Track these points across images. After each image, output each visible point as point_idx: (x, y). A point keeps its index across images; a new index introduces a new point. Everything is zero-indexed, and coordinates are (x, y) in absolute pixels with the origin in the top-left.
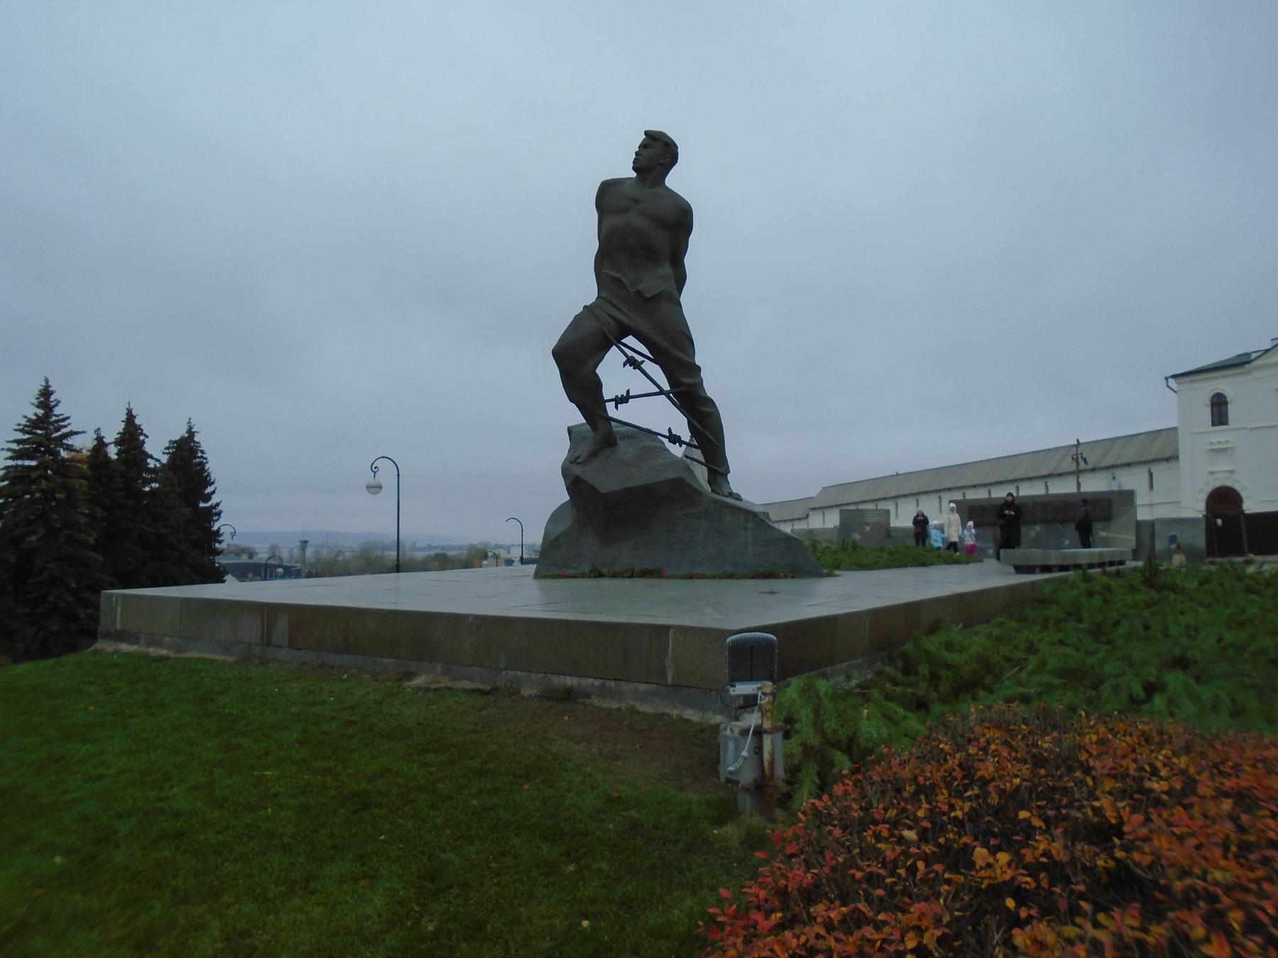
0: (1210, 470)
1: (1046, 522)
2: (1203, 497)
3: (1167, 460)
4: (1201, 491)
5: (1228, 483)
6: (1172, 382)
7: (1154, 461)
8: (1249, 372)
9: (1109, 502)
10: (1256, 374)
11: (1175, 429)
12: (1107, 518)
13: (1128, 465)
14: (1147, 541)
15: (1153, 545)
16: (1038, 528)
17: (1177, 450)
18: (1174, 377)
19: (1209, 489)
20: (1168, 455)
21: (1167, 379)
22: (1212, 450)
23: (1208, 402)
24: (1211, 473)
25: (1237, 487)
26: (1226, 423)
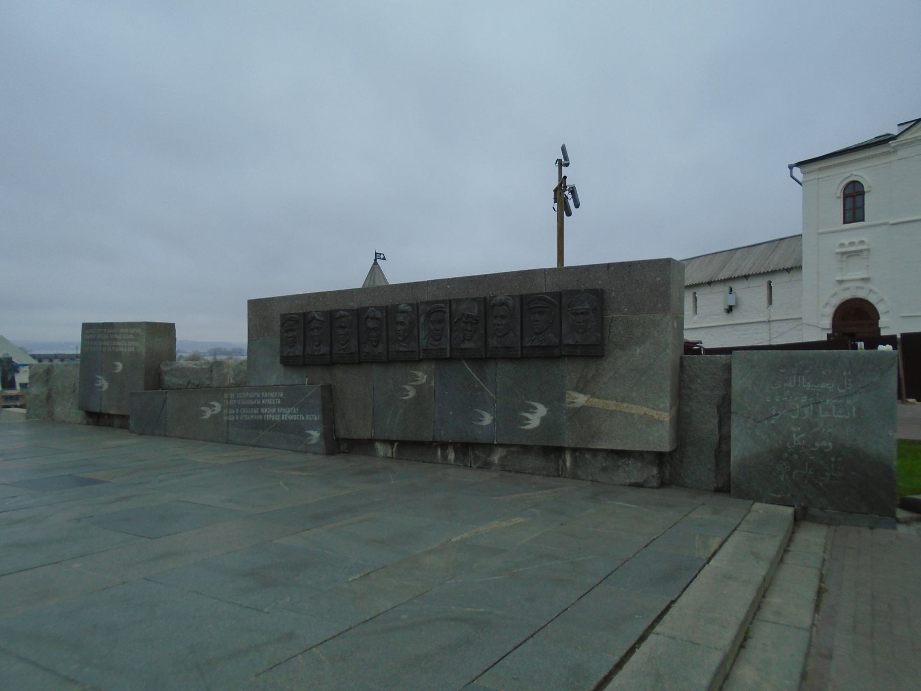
0: (839, 278)
1: (439, 359)
2: (830, 311)
3: (788, 270)
4: (827, 304)
5: (861, 294)
6: (797, 171)
7: (774, 272)
8: (895, 151)
9: (599, 296)
10: (901, 153)
11: (801, 235)
12: (593, 352)
13: (746, 277)
14: (706, 423)
15: (725, 438)
16: (422, 376)
17: (800, 259)
18: (799, 164)
19: (836, 302)
20: (789, 265)
21: (791, 167)
22: (843, 254)
23: (840, 193)
24: (841, 282)
25: (872, 299)
26: (863, 220)
